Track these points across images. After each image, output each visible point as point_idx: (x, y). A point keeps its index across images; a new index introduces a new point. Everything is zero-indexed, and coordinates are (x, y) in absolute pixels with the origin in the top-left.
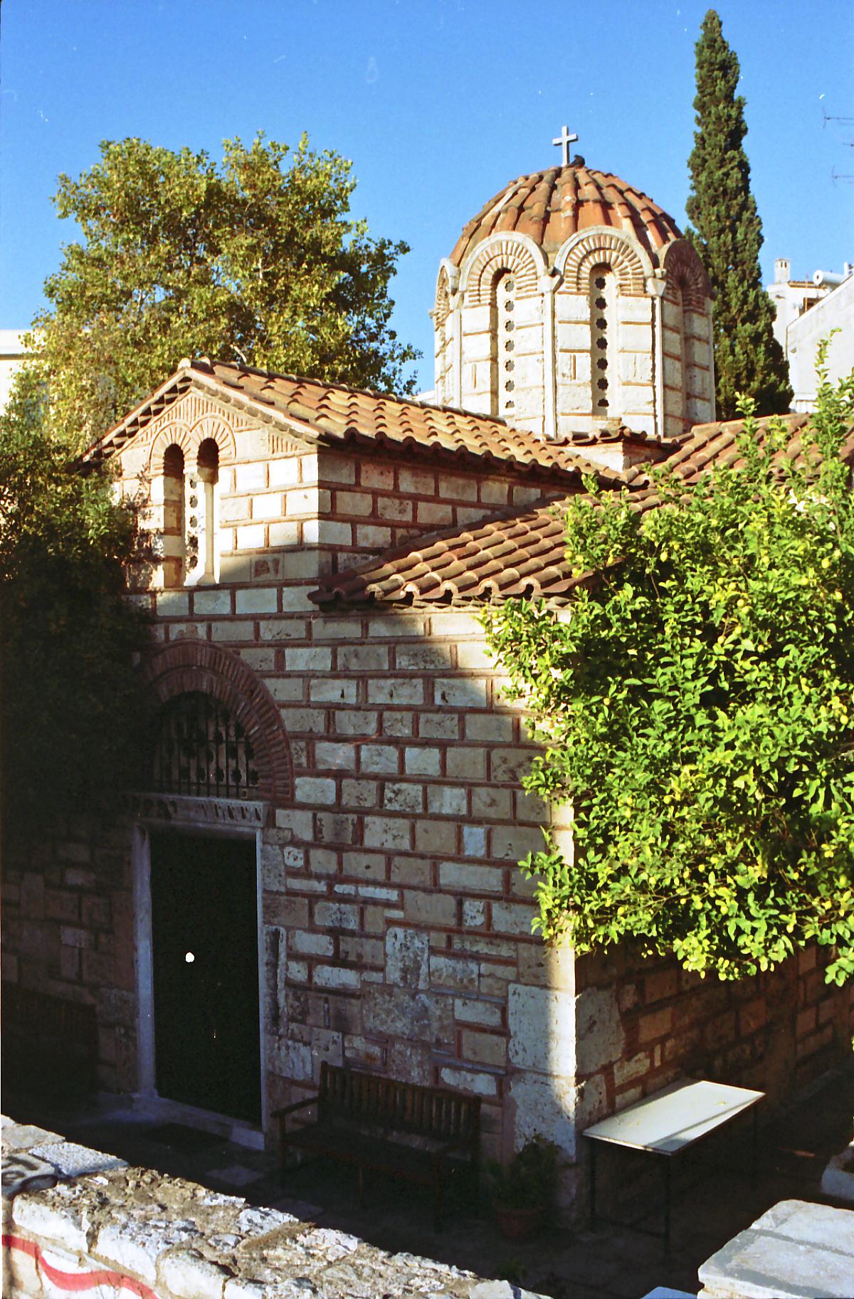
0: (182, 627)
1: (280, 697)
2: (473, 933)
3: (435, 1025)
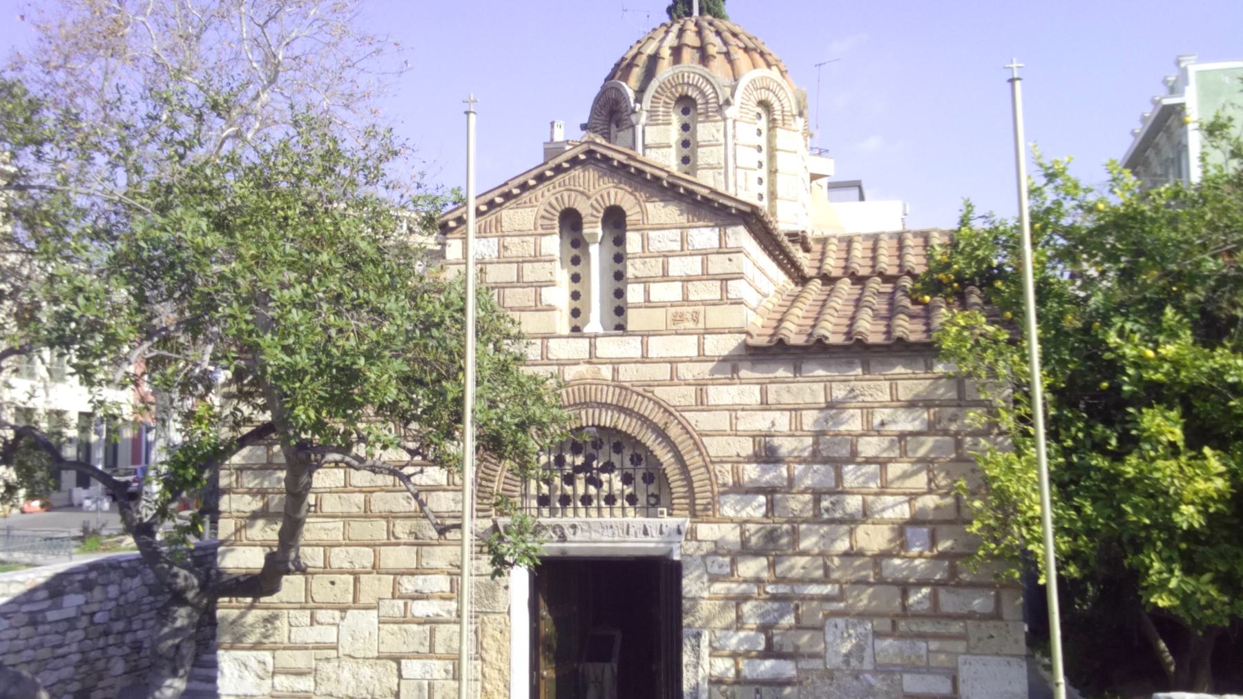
0: (583, 369)
1: (701, 427)
2: (918, 616)
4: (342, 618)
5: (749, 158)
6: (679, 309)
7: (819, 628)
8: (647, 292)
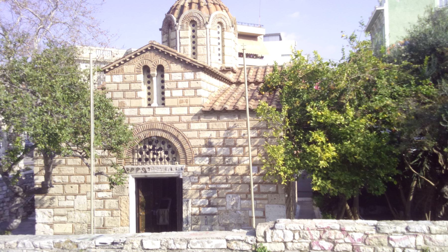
0: (151, 118)
1: (189, 136)
3: (243, 219)
4: (75, 198)
5: (215, 42)
6: (182, 99)
7: (224, 198)
8: (171, 93)
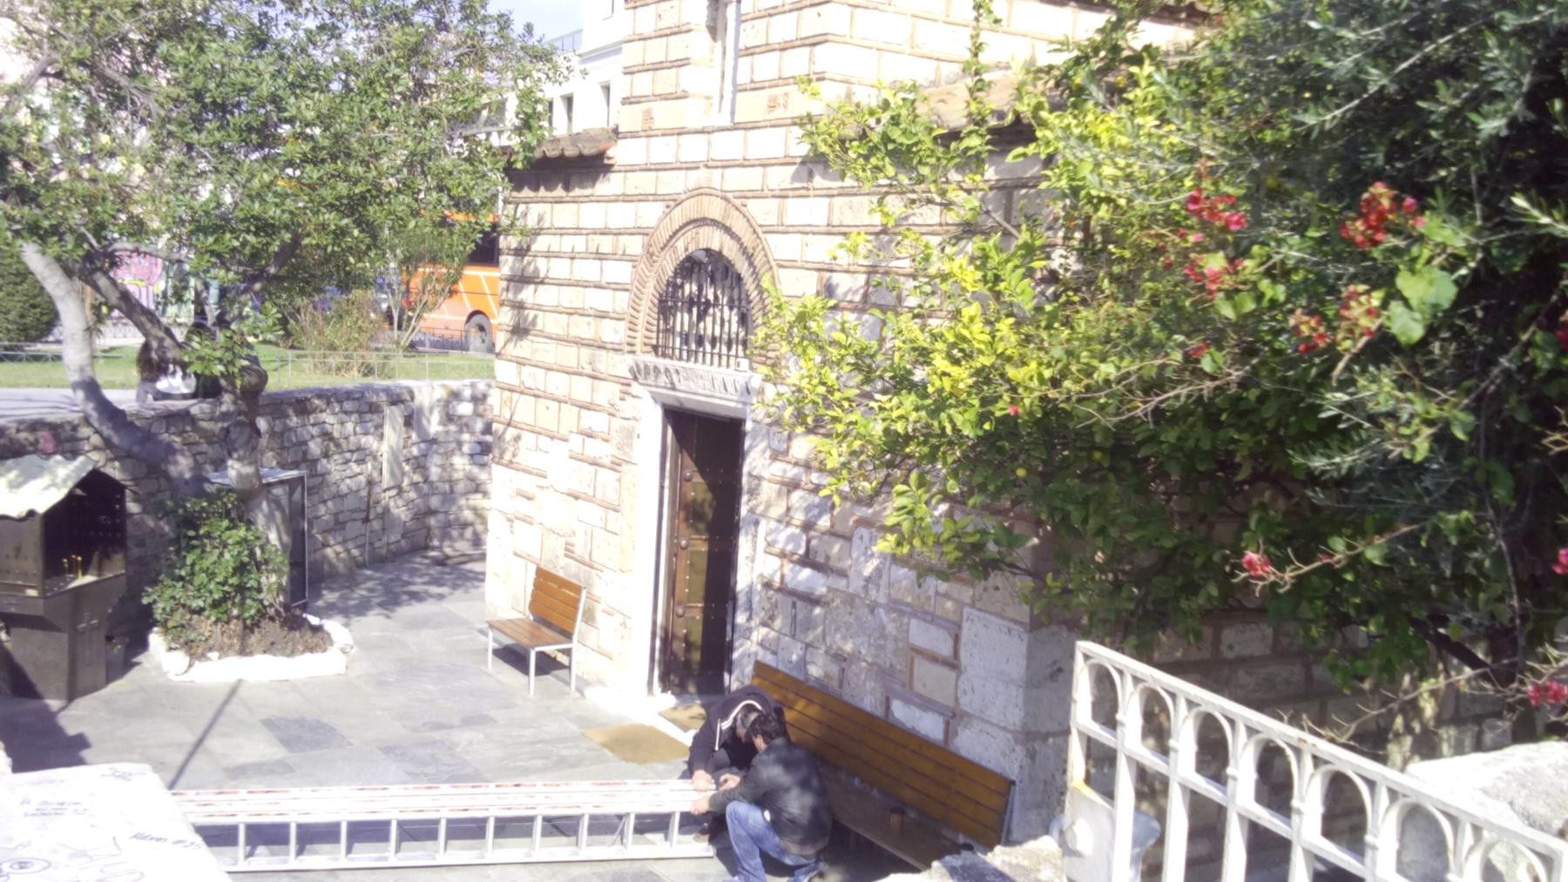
7: (847, 538)
